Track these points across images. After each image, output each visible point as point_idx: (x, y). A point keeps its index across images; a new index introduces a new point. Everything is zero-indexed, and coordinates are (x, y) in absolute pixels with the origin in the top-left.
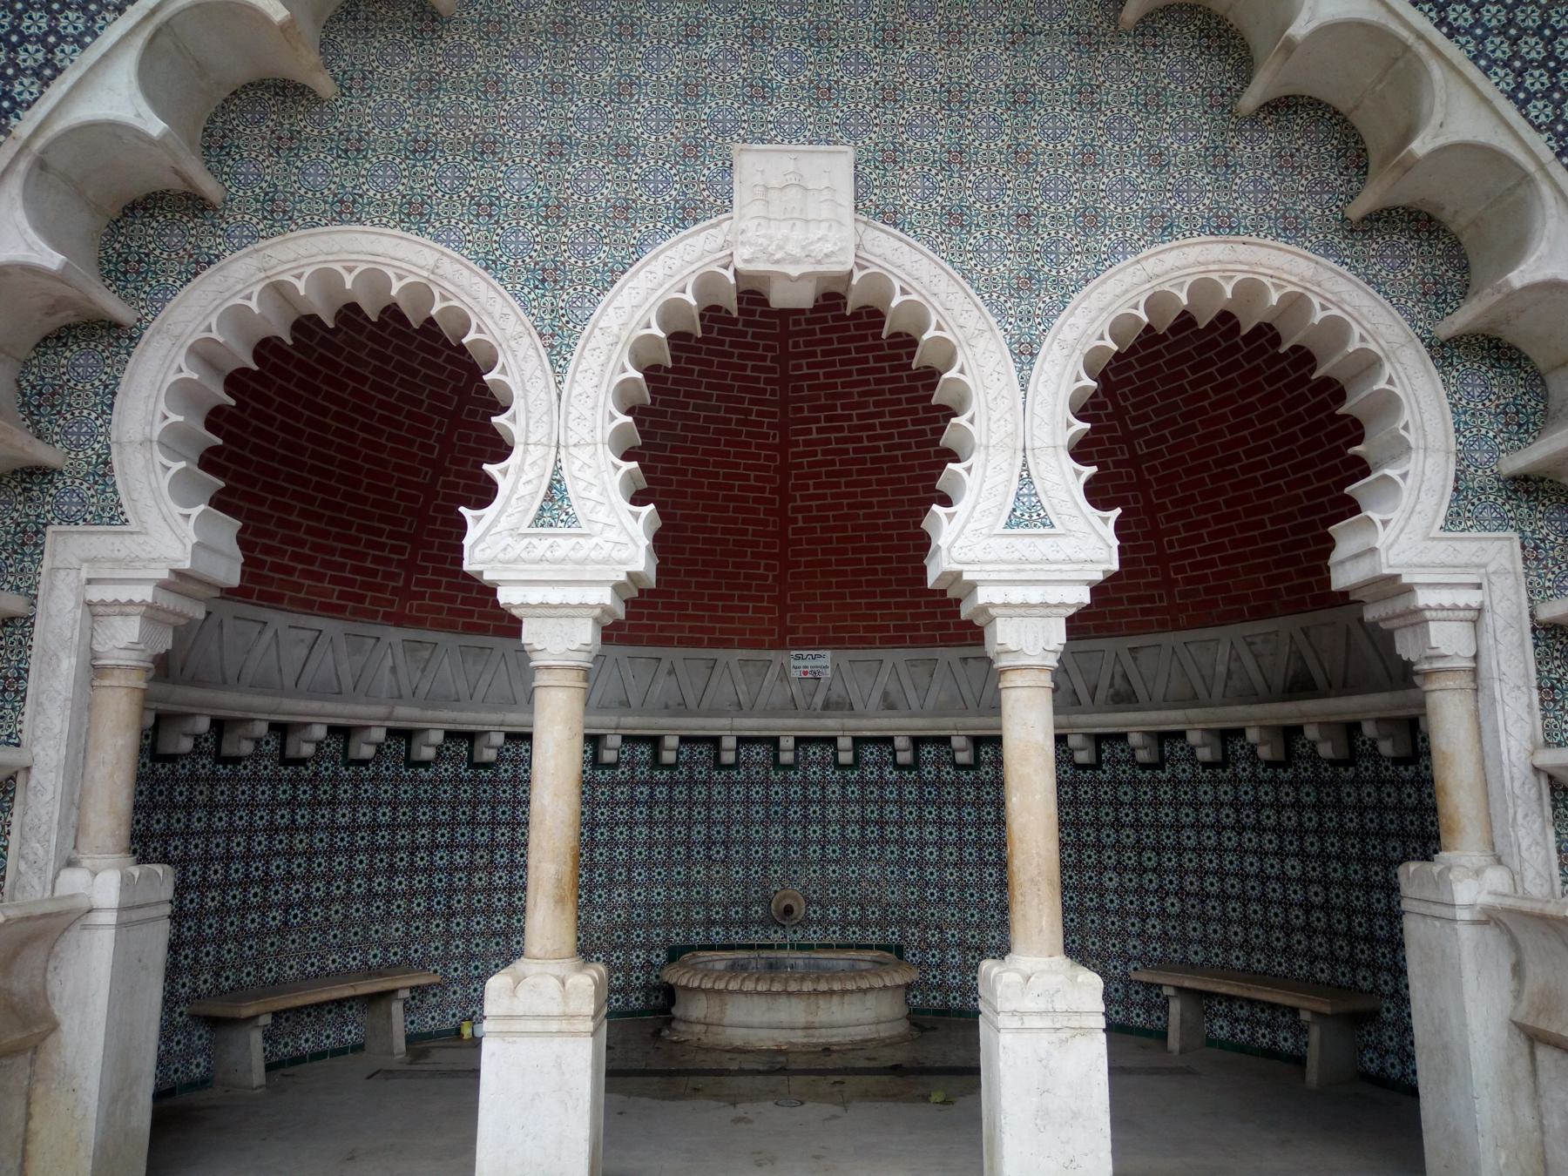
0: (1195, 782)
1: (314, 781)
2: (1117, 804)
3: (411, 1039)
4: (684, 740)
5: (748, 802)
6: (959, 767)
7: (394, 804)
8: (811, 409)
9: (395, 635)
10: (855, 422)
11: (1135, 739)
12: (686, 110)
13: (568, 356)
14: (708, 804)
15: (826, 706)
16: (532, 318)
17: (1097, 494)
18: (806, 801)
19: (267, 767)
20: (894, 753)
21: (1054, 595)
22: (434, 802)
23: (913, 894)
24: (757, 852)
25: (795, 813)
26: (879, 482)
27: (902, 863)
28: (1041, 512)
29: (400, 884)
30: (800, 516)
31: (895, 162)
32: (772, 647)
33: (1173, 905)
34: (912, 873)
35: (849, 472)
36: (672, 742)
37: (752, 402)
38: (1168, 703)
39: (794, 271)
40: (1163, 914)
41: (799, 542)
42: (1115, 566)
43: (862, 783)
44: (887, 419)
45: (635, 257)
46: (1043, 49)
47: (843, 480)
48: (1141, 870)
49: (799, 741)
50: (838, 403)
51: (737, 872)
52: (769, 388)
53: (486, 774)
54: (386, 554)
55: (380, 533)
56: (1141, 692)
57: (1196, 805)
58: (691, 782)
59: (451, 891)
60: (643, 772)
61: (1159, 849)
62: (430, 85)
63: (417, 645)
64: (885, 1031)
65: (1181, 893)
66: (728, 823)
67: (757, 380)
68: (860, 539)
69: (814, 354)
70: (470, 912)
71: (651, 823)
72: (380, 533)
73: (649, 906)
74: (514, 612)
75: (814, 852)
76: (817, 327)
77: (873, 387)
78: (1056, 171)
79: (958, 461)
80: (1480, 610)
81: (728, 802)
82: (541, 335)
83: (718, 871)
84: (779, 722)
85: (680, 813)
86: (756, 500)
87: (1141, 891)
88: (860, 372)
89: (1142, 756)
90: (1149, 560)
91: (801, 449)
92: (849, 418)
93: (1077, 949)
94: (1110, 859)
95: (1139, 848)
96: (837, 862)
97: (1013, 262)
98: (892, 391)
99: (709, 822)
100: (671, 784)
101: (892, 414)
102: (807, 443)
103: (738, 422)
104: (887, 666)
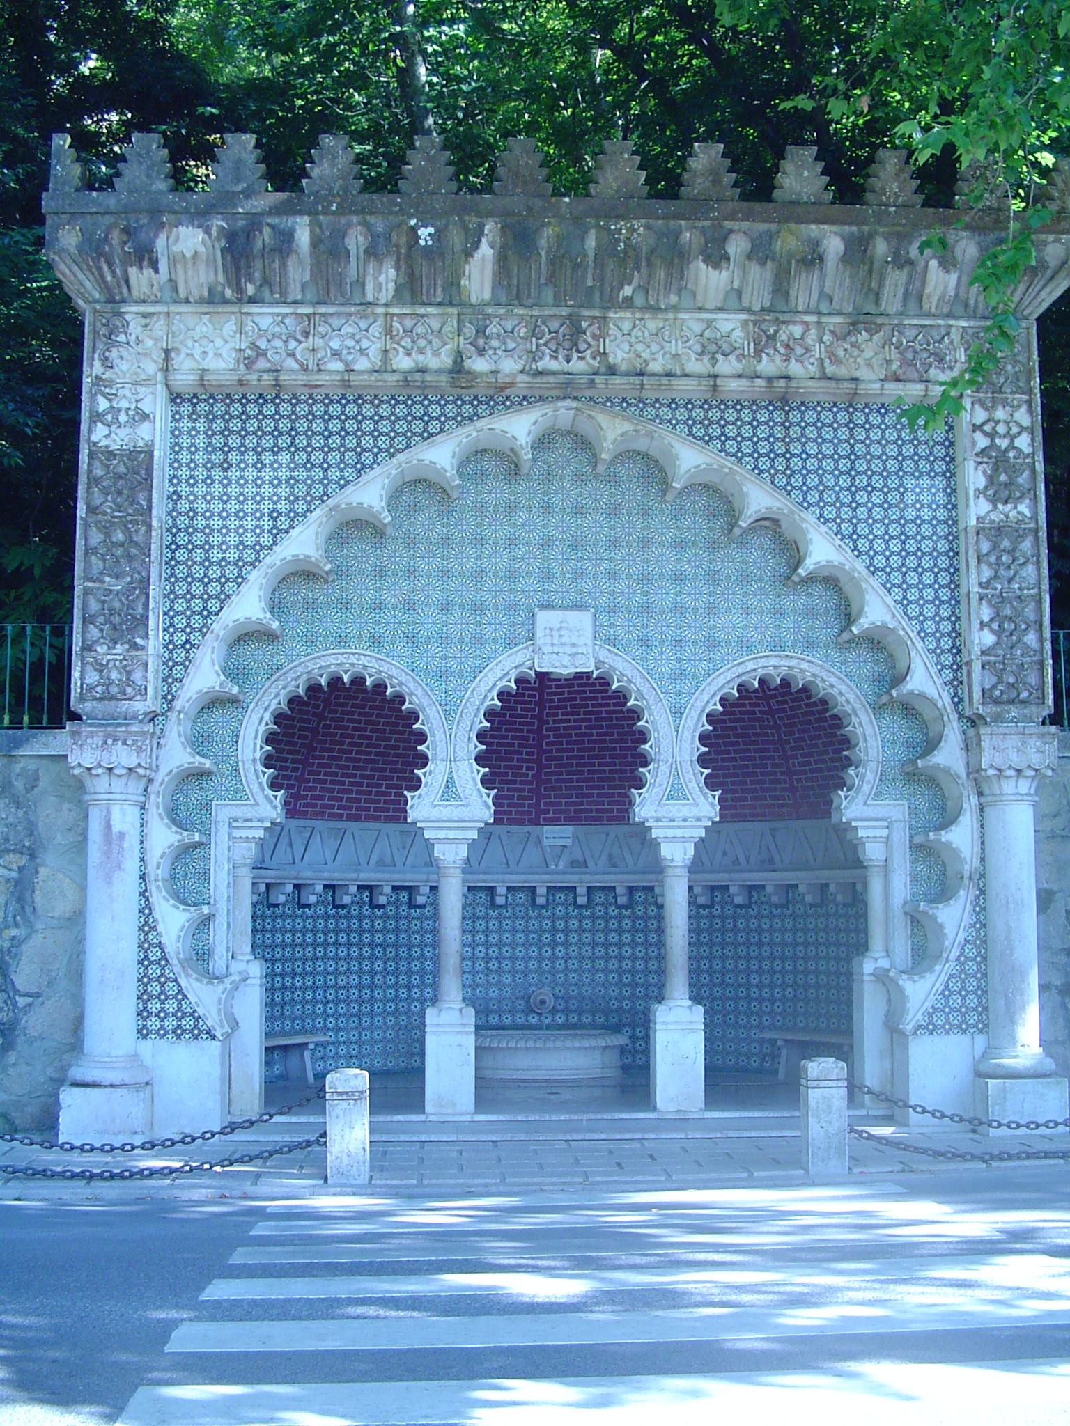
0: (805, 916)
5: (514, 930)
7: (293, 932)
11: (769, 889)
14: (486, 932)
17: (711, 783)
18: (554, 931)
20: (615, 898)
21: (687, 833)
22: (314, 930)
23: (627, 992)
24: (520, 965)
25: (546, 939)
27: (621, 972)
34: (627, 978)
39: (565, 672)
40: (784, 999)
42: (717, 819)
43: (593, 918)
46: (691, 551)
51: (506, 979)
53: (343, 912)
56: (777, 859)
57: (805, 930)
59: (326, 987)
61: (783, 958)
62: (380, 573)
64: (609, 1073)
66: (500, 945)
68: (593, 749)
70: (337, 1001)
75: (560, 965)
80: (887, 838)
81: (500, 931)
83: (493, 978)
84: (537, 877)
86: (521, 723)
87: (772, 986)
89: (775, 899)
90: (782, 773)
93: (696, 999)
96: (575, 971)
97: (674, 665)
99: (487, 945)
104: (612, 836)
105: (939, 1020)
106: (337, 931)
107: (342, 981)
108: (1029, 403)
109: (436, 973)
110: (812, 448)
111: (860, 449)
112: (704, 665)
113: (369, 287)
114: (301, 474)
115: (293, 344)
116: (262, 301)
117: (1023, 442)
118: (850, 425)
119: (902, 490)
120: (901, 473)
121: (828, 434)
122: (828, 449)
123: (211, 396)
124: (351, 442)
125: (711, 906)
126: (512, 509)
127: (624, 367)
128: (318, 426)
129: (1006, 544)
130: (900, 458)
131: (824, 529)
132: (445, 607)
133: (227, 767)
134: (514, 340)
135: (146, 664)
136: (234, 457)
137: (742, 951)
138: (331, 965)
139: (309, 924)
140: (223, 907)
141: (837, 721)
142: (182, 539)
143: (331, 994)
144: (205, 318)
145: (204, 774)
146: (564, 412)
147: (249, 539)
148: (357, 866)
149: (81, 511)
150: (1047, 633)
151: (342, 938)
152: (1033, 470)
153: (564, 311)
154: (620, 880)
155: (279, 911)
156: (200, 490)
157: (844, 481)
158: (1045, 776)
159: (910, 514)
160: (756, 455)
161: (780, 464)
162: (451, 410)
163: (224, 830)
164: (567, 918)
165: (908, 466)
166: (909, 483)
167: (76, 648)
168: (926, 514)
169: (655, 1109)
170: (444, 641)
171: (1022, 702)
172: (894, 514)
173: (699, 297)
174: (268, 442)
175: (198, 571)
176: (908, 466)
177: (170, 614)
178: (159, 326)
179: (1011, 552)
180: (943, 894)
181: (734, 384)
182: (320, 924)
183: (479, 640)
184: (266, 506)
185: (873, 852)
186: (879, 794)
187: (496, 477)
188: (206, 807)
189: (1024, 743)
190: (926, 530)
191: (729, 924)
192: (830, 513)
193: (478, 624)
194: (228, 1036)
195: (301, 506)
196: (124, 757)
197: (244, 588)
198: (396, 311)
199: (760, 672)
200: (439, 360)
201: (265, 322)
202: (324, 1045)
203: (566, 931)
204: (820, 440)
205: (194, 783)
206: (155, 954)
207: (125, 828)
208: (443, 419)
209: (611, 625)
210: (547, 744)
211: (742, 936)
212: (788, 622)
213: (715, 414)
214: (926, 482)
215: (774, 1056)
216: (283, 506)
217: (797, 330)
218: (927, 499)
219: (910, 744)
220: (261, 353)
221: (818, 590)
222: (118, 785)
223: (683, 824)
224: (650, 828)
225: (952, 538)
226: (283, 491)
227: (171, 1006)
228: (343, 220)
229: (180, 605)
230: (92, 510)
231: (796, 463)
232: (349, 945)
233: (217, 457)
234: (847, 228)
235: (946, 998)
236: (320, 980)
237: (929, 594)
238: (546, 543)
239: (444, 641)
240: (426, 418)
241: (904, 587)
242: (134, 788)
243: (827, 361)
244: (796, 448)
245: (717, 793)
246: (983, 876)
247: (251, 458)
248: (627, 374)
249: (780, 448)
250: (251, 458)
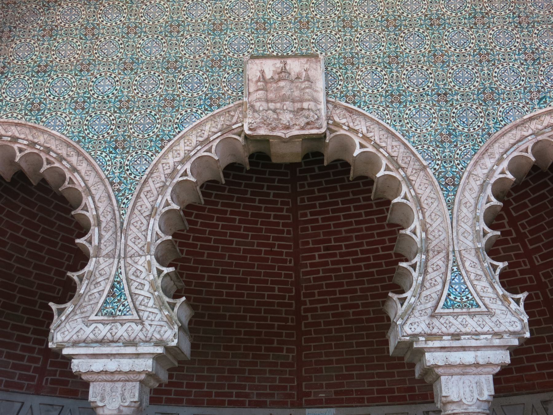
8: (314, 242)
10: (344, 250)
12: (214, 39)
13: (130, 197)
16: (107, 173)
21: (483, 357)
26: (362, 290)
28: (469, 296)
30: (309, 315)
31: (353, 64)
35: (342, 284)
37: (275, 239)
41: (309, 333)
42: (528, 335)
44: (365, 247)
45: (177, 131)
47: (337, 289)
50: (332, 237)
52: (286, 229)
54: (31, 344)
55: (26, 330)
63: (49, 407)
67: (278, 224)
69: (314, 206)
72: (26, 330)
74: (84, 377)
76: (316, 189)
77: (354, 226)
78: (462, 66)
79: (407, 260)
82: (112, 184)
88: (345, 217)
91: (309, 269)
92: (340, 247)
98: (367, 229)
101: (368, 244)
102: (312, 265)
103: (266, 252)
210: (307, 325)
223: (474, 343)
224: (421, 352)
245: (522, 296)
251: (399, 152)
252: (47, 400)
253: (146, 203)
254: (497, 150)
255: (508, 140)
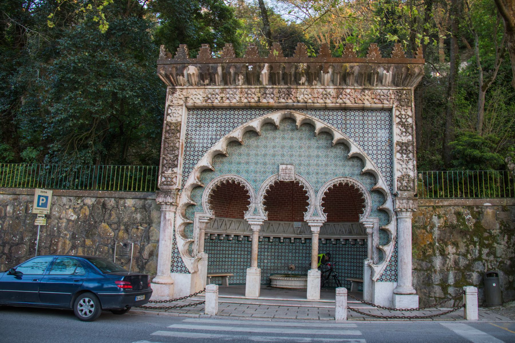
0: (360, 248)
1: (215, 243)
2: (348, 251)
3: (229, 284)
4: (274, 238)
5: (285, 249)
6: (323, 244)
7: (226, 247)
9: (226, 219)
11: (350, 240)
14: (278, 249)
15: (300, 232)
17: (325, 211)
18: (296, 249)
19: (209, 240)
21: (318, 224)
22: (232, 247)
24: (287, 258)
25: (294, 251)
29: (227, 260)
32: (291, 221)
33: (355, 268)
36: (272, 238)
38: (357, 234)
39: (287, 181)
40: (354, 270)
43: (306, 246)
46: (321, 150)
48: (351, 262)
49: (295, 238)
51: (283, 261)
58: (275, 245)
59: (234, 261)
60: (266, 243)
61: (354, 259)
62: (240, 154)
65: (356, 266)
66: (282, 252)
70: (237, 265)
71: (268, 252)
73: (267, 266)
75: (297, 258)
80: (373, 227)
81: (282, 249)
83: (280, 261)
85: (273, 250)
87: (351, 266)
89: (352, 243)
93: (319, 268)
94: (347, 260)
95: (351, 259)
97: (316, 179)
99: (278, 252)
100: (272, 245)
105: (384, 277)
106: (238, 247)
107: (239, 260)
108: (411, 110)
109: (251, 259)
110: (352, 122)
111: (366, 122)
112: (324, 180)
113: (237, 81)
114: (219, 129)
115: (217, 96)
116: (210, 85)
117: (410, 120)
118: (363, 116)
119: (377, 133)
120: (377, 129)
121: (357, 118)
122: (357, 122)
123: (198, 109)
124: (232, 121)
125: (326, 244)
126: (274, 138)
127: (302, 101)
128: (224, 117)
129: (404, 148)
130: (377, 124)
131: (355, 143)
132: (256, 163)
133: (199, 203)
134: (273, 94)
135: (176, 177)
136: (202, 125)
137: (344, 256)
138: (236, 256)
139: (230, 245)
140: (196, 240)
141: (361, 195)
142: (188, 145)
143: (236, 263)
144: (196, 90)
145: (193, 205)
146: (286, 112)
147: (205, 145)
148: (244, 231)
149: (163, 138)
150: (416, 171)
151: (239, 249)
152: (412, 127)
153: (286, 87)
154: (303, 236)
155: (222, 241)
156: (194, 133)
157: (361, 131)
158: (414, 211)
159: (379, 139)
160: (337, 124)
161: (344, 126)
162: (257, 112)
163: (197, 219)
164: (299, 246)
165: (379, 126)
166: (379, 131)
167: (160, 172)
168: (383, 139)
169: (306, 297)
170: (256, 172)
171: (408, 190)
172: (375, 139)
173: (322, 82)
174: (211, 121)
175: (192, 153)
176: (379, 126)
177: (185, 164)
178: (184, 92)
179: (406, 150)
180: (387, 243)
181: (331, 105)
182: (234, 245)
183: (265, 172)
184: (210, 137)
185: (369, 231)
186: (371, 215)
187: (271, 130)
188: (193, 213)
189: (408, 202)
190: (383, 144)
191: (341, 249)
192: (357, 139)
193: (264, 168)
194: (195, 272)
195: (218, 137)
196: (169, 200)
197: (203, 158)
198: (243, 87)
199: (339, 182)
200: (253, 100)
201: (211, 91)
202: (233, 276)
203: (299, 249)
204: (355, 120)
205: (191, 207)
206: (176, 251)
207: (169, 218)
208: (255, 115)
209: (299, 169)
211: (344, 253)
212: (347, 168)
213: (327, 113)
214: (383, 131)
215: (351, 285)
216: (214, 137)
217: (348, 91)
218: (383, 135)
219: (379, 202)
220: (209, 98)
221: (355, 160)
222: (168, 207)
225: (391, 145)
226: (214, 133)
227: (179, 264)
228: (230, 64)
229: (187, 162)
230: (166, 138)
231: (348, 126)
232: (241, 251)
233: (198, 125)
234: (361, 64)
235: (386, 272)
236: (233, 260)
237: (384, 161)
238: (283, 147)
239: (256, 172)
240: (251, 115)
241: (377, 159)
242: (173, 209)
243: (356, 99)
244: (348, 122)
245: (327, 214)
246: (397, 238)
247: (206, 125)
248: (303, 103)
249: (344, 122)
250: (206, 125)
251: (308, 185)
252: (229, 219)
253: (260, 193)
254: (326, 186)
255: (328, 184)
